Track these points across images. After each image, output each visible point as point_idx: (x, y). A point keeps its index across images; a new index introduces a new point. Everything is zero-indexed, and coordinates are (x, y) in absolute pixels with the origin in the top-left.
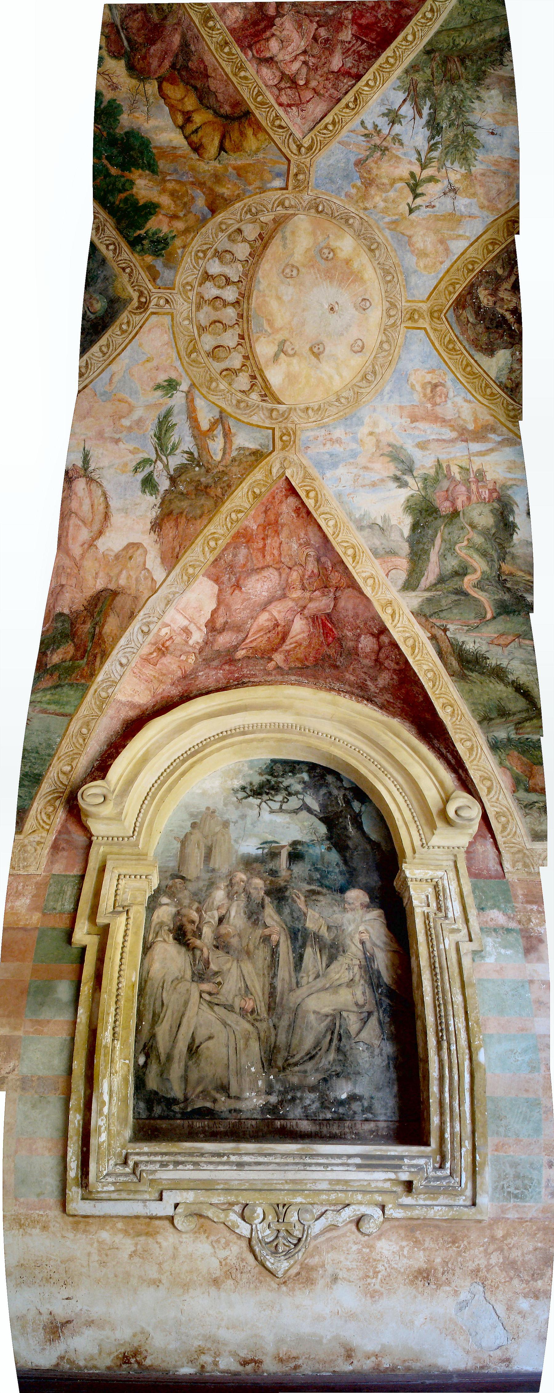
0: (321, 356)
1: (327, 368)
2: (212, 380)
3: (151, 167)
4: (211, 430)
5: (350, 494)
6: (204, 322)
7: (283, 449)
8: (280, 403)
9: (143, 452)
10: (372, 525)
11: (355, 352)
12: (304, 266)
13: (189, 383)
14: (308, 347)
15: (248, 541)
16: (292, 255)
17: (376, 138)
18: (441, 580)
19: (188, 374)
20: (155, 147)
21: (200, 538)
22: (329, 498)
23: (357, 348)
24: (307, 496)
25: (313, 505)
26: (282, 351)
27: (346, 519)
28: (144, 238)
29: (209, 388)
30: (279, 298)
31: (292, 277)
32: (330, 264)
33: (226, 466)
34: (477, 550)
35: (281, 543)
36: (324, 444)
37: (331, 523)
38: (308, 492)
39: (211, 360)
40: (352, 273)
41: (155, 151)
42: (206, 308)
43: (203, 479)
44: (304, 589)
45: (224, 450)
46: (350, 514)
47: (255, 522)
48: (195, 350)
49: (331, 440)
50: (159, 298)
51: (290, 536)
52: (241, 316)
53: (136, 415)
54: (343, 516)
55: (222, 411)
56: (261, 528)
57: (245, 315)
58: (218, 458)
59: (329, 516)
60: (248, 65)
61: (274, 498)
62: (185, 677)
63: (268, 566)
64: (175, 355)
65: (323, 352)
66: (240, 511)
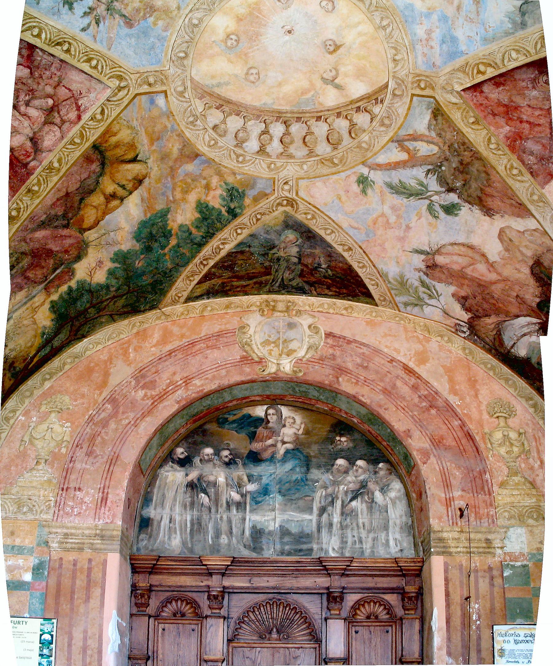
0: (338, 43)
1: (350, 38)
2: (359, 147)
3: (164, 214)
4: (408, 151)
5: (486, 30)
6: (305, 151)
7: (433, 89)
8: (386, 86)
11: (334, 8)
12: (246, 63)
16: (236, 76)
17: (99, 10)
19: (354, 167)
20: (145, 215)
26: (333, 81)
28: (229, 208)
30: (280, 85)
31: (258, 74)
32: (243, 38)
36: (432, 47)
37: (514, 55)
39: (340, 147)
40: (251, 14)
41: (149, 215)
42: (292, 150)
45: (428, 142)
46: (507, 34)
48: (331, 160)
49: (427, 40)
50: (282, 189)
52: (299, 119)
53: (387, 209)
55: (392, 140)
59: (506, 56)
60: (45, 163)
64: (335, 177)
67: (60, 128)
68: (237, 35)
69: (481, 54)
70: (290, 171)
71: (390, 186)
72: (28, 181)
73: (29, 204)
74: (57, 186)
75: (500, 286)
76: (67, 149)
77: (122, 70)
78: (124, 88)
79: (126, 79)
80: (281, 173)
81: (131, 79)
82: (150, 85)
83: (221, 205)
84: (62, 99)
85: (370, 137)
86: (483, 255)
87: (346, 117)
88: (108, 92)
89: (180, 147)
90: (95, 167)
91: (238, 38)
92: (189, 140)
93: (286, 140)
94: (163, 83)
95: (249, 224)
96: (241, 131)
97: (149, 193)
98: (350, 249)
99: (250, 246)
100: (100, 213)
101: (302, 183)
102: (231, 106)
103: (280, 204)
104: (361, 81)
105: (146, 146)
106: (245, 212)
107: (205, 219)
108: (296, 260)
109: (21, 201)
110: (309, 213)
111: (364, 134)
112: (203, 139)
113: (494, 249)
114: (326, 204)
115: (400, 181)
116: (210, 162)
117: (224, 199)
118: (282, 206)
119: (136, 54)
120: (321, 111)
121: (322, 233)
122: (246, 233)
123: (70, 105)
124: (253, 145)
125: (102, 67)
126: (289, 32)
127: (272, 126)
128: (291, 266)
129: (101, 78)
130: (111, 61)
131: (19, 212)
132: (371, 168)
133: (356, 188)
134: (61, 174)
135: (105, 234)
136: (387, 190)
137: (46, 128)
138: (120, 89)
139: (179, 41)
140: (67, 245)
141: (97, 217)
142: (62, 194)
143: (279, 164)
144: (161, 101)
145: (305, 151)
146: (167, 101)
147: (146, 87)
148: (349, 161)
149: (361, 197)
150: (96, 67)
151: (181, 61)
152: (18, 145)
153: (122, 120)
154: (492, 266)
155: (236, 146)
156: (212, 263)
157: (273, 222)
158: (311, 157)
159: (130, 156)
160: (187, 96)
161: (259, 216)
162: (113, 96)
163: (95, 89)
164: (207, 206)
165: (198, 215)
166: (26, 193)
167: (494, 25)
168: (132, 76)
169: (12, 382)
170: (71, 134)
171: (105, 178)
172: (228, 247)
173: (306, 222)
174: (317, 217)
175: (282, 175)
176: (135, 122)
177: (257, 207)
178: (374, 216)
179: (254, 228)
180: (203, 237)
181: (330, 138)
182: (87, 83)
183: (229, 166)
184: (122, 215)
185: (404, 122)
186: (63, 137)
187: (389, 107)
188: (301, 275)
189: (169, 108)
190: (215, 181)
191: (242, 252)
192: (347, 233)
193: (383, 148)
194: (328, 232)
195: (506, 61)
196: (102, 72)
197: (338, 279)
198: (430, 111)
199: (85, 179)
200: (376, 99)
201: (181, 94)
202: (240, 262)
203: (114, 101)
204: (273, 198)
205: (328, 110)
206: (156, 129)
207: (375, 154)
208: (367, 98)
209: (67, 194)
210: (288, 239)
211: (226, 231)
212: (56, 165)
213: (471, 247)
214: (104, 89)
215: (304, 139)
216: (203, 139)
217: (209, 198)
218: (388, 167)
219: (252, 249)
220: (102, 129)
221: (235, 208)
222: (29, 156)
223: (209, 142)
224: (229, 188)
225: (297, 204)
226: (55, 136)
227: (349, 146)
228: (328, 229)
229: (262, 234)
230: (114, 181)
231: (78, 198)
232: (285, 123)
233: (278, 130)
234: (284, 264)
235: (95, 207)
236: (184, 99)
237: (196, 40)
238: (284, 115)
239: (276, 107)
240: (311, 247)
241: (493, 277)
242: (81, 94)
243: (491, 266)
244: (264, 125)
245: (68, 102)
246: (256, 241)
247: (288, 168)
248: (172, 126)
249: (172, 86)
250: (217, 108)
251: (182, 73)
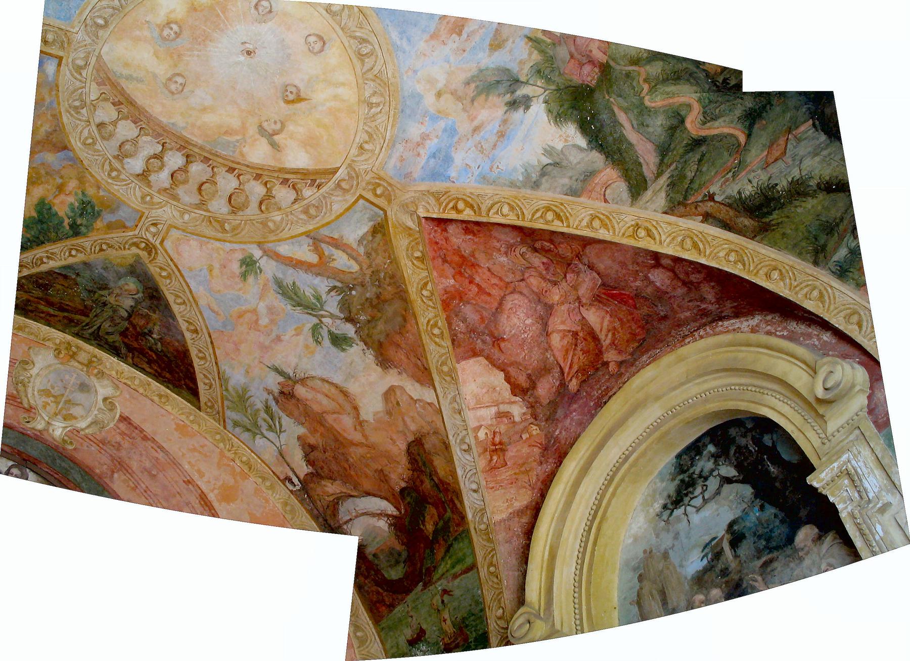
0: (303, 95)
1: (321, 95)
2: (264, 224)
6: (196, 199)
7: (389, 201)
9: (304, 325)
10: (544, 171)
11: (322, 50)
13: (255, 246)
14: (282, 104)
15: (461, 299)
18: (664, 151)
19: (245, 243)
21: (423, 337)
22: (478, 192)
23: (318, 47)
24: (459, 212)
25: (472, 213)
27: (513, 192)
29: (271, 231)
30: (204, 110)
33: (370, 266)
34: (665, 81)
35: (489, 270)
37: (506, 210)
38: (455, 208)
39: (241, 213)
42: (180, 191)
43: (368, 295)
44: (555, 283)
46: (512, 184)
47: (447, 278)
48: (222, 223)
51: (489, 256)
52: (206, 160)
53: (262, 307)
54: (508, 192)
55: (307, 234)
56: (457, 276)
57: (206, 155)
58: (355, 267)
59: (496, 206)
61: (437, 243)
62: (545, 449)
63: (503, 298)
64: (218, 244)
65: (299, 90)
66: (426, 284)
69: (469, 191)
70: (167, 213)
71: (279, 284)
75: (360, 451)
83: (67, 215)
85: (282, 219)
86: (356, 408)
87: (266, 184)
93: (178, 176)
98: (196, 331)
99: (78, 275)
103: (136, 245)
104: (307, 152)
106: (90, 234)
107: (41, 221)
108: (125, 314)
110: (165, 270)
111: (277, 213)
113: (372, 406)
114: (191, 269)
115: (294, 283)
116: (76, 161)
117: (73, 210)
118: (138, 247)
120: (238, 163)
121: (171, 299)
122: (81, 257)
124: (136, 165)
126: (249, 53)
128: (116, 318)
132: (266, 253)
133: (236, 267)
136: (272, 286)
143: (156, 200)
145: (195, 199)
148: (243, 233)
149: (237, 280)
154: (361, 424)
157: (119, 260)
158: (199, 209)
161: (104, 247)
164: (50, 209)
165: (35, 214)
167: (504, 168)
173: (157, 278)
174: (174, 279)
175: (154, 213)
177: (107, 236)
178: (244, 308)
179: (93, 256)
181: (233, 198)
183: (96, 175)
185: (333, 221)
187: (325, 197)
188: (123, 334)
190: (72, 185)
191: (66, 277)
192: (201, 313)
193: (292, 237)
194: (179, 301)
195: (492, 211)
197: (166, 359)
198: (371, 223)
200: (314, 181)
202: (59, 287)
205: (248, 166)
207: (279, 241)
208: (303, 174)
210: (126, 287)
213: (345, 393)
215: (202, 185)
217: (57, 201)
218: (288, 262)
219: (79, 279)
221: (81, 225)
223: (86, 139)
224: (85, 200)
225: (156, 253)
227: (252, 218)
228: (180, 297)
233: (175, 160)
234: (108, 312)
239: (185, 134)
240: (150, 308)
241: (357, 437)
243: (360, 424)
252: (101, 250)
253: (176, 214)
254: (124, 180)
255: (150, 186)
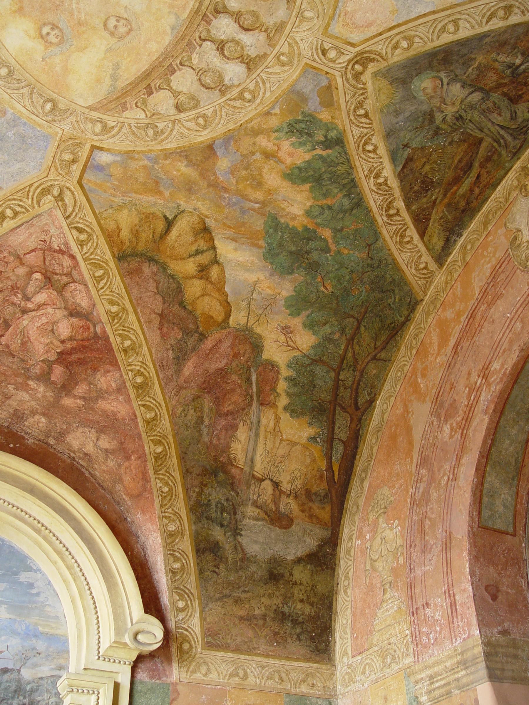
16: (109, 50)
67: (74, 281)
68: (45, 24)
70: (305, 38)
72: (113, 345)
73: (141, 360)
74: (142, 320)
76: (102, 288)
77: (36, 185)
78: (61, 193)
79: (51, 186)
80: (303, 52)
81: (55, 180)
82: (74, 161)
83: (309, 151)
84: (40, 263)
88: (58, 213)
89: (185, 162)
90: (147, 269)
91: (49, 24)
92: (180, 148)
93: (248, 22)
94: (81, 145)
95: (365, 131)
96: (203, 77)
97: (230, 227)
99: (406, 146)
100: (216, 295)
101: (337, 28)
102: (154, 75)
103: (357, 76)
105: (159, 201)
106: (340, 127)
109: (131, 365)
112: (189, 129)
116: (229, 138)
118: (362, 73)
119: (22, 160)
122: (378, 140)
123: (54, 258)
124: (233, 71)
125: (19, 205)
127: (214, 32)
129: (33, 212)
130: (17, 192)
131: (142, 374)
134: (130, 309)
135: (249, 304)
137: (68, 295)
138: (60, 198)
139: (27, 103)
140: (229, 350)
141: (219, 300)
142: (157, 321)
143: (286, 49)
144: (104, 158)
146: (108, 150)
147: (74, 167)
150: (16, 214)
151: (56, 111)
152: (70, 330)
153: (105, 213)
155: (223, 93)
156: (400, 204)
157: (383, 97)
159: (161, 226)
160: (114, 124)
161: (361, 112)
162: (65, 210)
163: (46, 224)
164: (300, 169)
166: (126, 355)
168: (51, 177)
169: (328, 508)
170: (87, 277)
171: (172, 266)
172: (388, 172)
176: (116, 200)
180: (348, 195)
182: (32, 230)
184: (238, 273)
186: (86, 286)
189: (119, 153)
190: (263, 142)
196: (26, 209)
199: (157, 288)
201: (106, 129)
203: (73, 211)
204: (339, 80)
206: (141, 180)
209: (161, 315)
211: (357, 163)
212: (114, 309)
214: (50, 215)
216: (189, 129)
217: (289, 161)
220: (102, 241)
221: (326, 137)
222: (89, 328)
223: (198, 124)
224: (286, 129)
225: (370, 52)
226: (80, 291)
229: (395, 120)
230: (183, 259)
231: (177, 306)
232: (217, 12)
235: (203, 295)
236: (116, 130)
237: (33, 81)
238: (204, 8)
242: (45, 241)
244: (209, 43)
245: (48, 258)
246: (402, 134)
247: (298, 39)
248: (148, 159)
249: (89, 135)
250: (150, 94)
251: (76, 117)
252: (366, 115)
253: (305, 26)
254: (257, 84)
255: (265, 56)
